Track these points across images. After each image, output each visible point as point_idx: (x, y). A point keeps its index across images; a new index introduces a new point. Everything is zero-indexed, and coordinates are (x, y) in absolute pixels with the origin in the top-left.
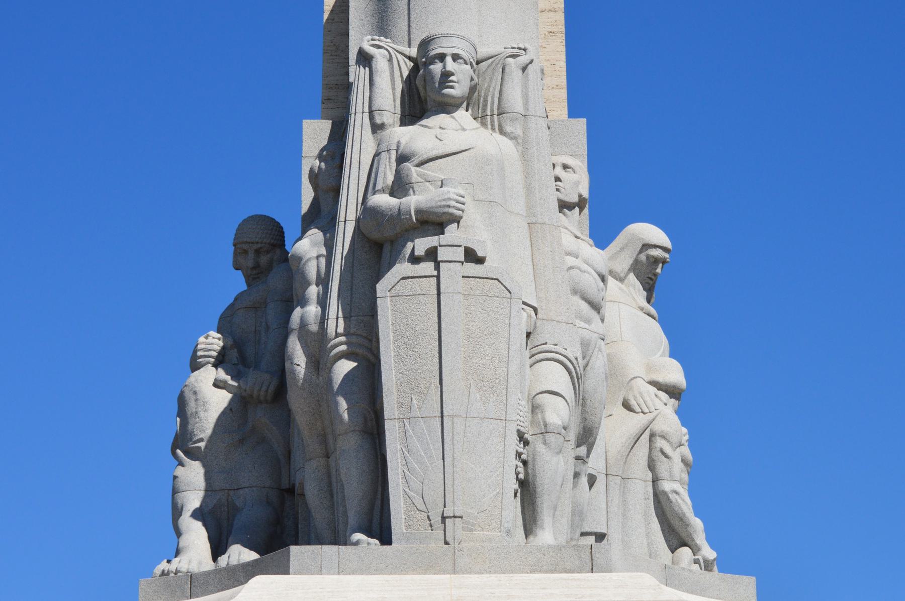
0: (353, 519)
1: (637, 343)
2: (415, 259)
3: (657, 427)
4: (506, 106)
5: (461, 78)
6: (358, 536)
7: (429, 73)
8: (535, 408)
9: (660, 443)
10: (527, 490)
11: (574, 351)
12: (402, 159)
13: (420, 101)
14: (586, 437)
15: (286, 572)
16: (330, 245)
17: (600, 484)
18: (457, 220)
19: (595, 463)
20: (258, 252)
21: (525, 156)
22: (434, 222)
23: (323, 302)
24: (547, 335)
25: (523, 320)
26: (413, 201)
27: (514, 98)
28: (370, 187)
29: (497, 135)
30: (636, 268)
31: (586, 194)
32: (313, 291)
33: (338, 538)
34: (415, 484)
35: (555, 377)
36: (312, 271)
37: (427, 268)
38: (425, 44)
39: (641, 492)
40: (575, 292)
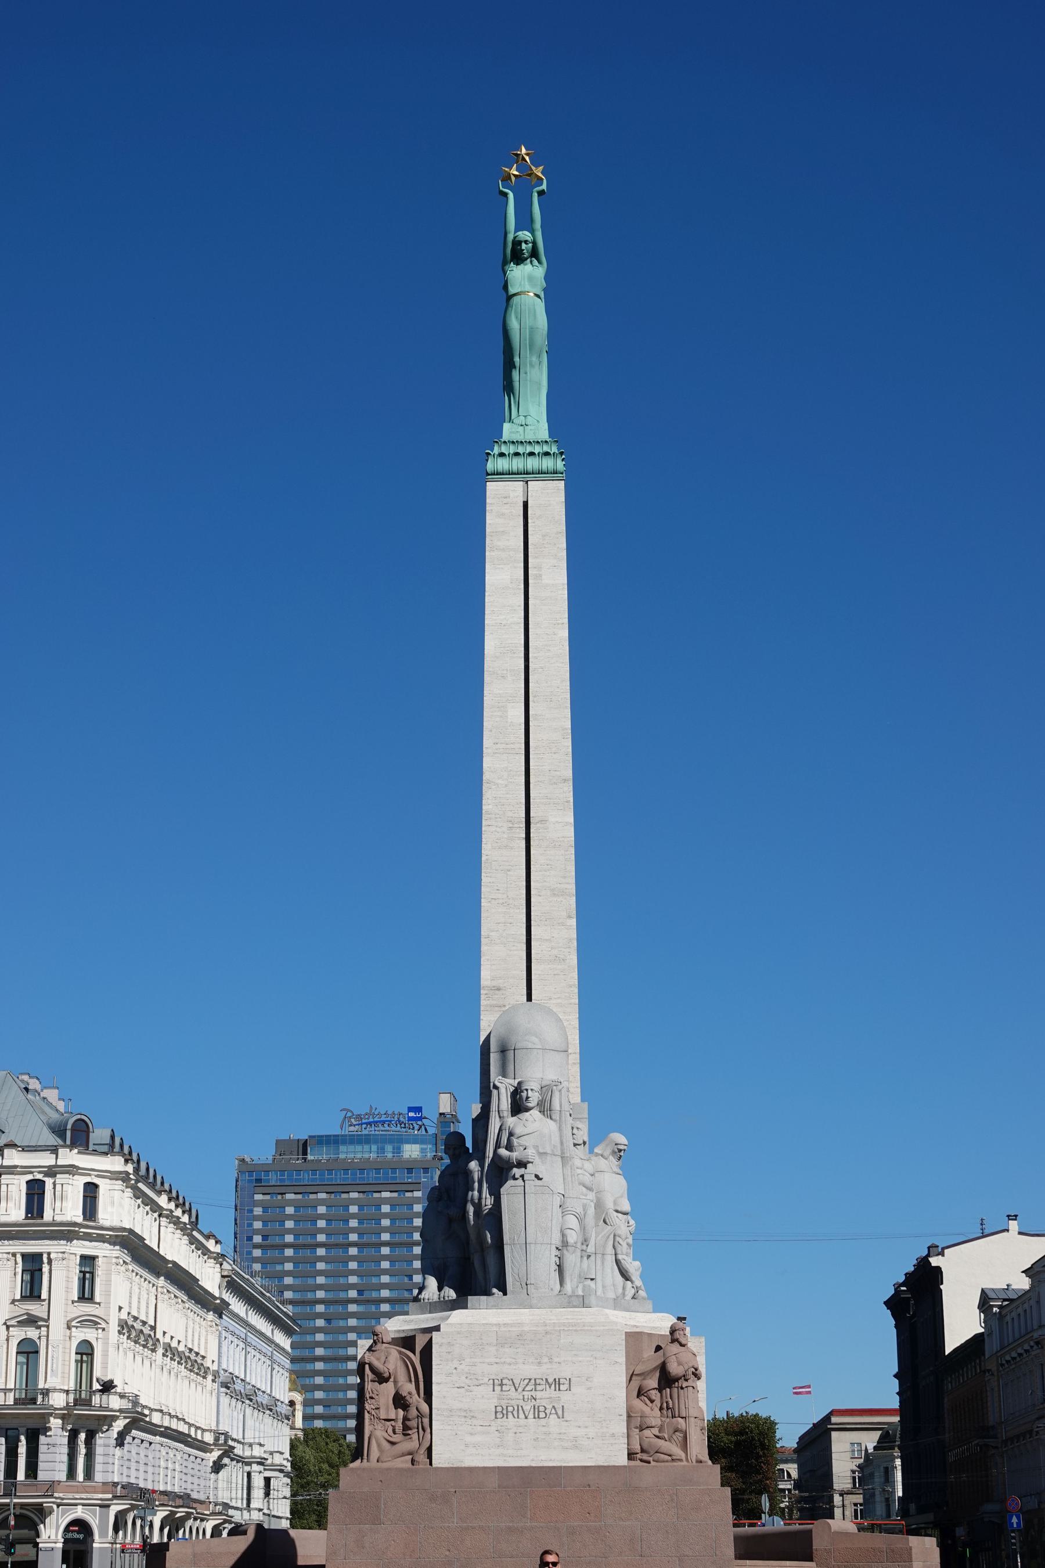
0: (492, 1283)
1: (614, 1186)
2: (515, 1178)
3: (619, 1232)
4: (553, 1108)
5: (534, 1098)
6: (495, 1290)
7: (521, 1097)
8: (563, 1235)
9: (618, 1239)
10: (560, 1268)
11: (580, 1210)
12: (511, 1134)
13: (518, 1107)
14: (585, 1241)
15: (466, 1308)
16: (482, 1166)
17: (592, 1258)
18: (505, 1294)
19: (591, 1249)
20: (455, 1149)
21: (560, 1129)
22: (522, 1164)
23: (480, 1191)
24: (569, 1204)
25: (558, 1200)
26: (515, 1155)
27: (556, 1105)
28: (498, 1145)
29: (549, 1120)
30: (614, 1152)
31: (586, 1139)
32: (476, 1185)
33: (488, 1293)
34: (516, 1271)
35: (572, 1222)
36: (476, 1178)
37: (520, 1182)
38: (520, 1083)
39: (610, 1259)
40: (580, 1184)
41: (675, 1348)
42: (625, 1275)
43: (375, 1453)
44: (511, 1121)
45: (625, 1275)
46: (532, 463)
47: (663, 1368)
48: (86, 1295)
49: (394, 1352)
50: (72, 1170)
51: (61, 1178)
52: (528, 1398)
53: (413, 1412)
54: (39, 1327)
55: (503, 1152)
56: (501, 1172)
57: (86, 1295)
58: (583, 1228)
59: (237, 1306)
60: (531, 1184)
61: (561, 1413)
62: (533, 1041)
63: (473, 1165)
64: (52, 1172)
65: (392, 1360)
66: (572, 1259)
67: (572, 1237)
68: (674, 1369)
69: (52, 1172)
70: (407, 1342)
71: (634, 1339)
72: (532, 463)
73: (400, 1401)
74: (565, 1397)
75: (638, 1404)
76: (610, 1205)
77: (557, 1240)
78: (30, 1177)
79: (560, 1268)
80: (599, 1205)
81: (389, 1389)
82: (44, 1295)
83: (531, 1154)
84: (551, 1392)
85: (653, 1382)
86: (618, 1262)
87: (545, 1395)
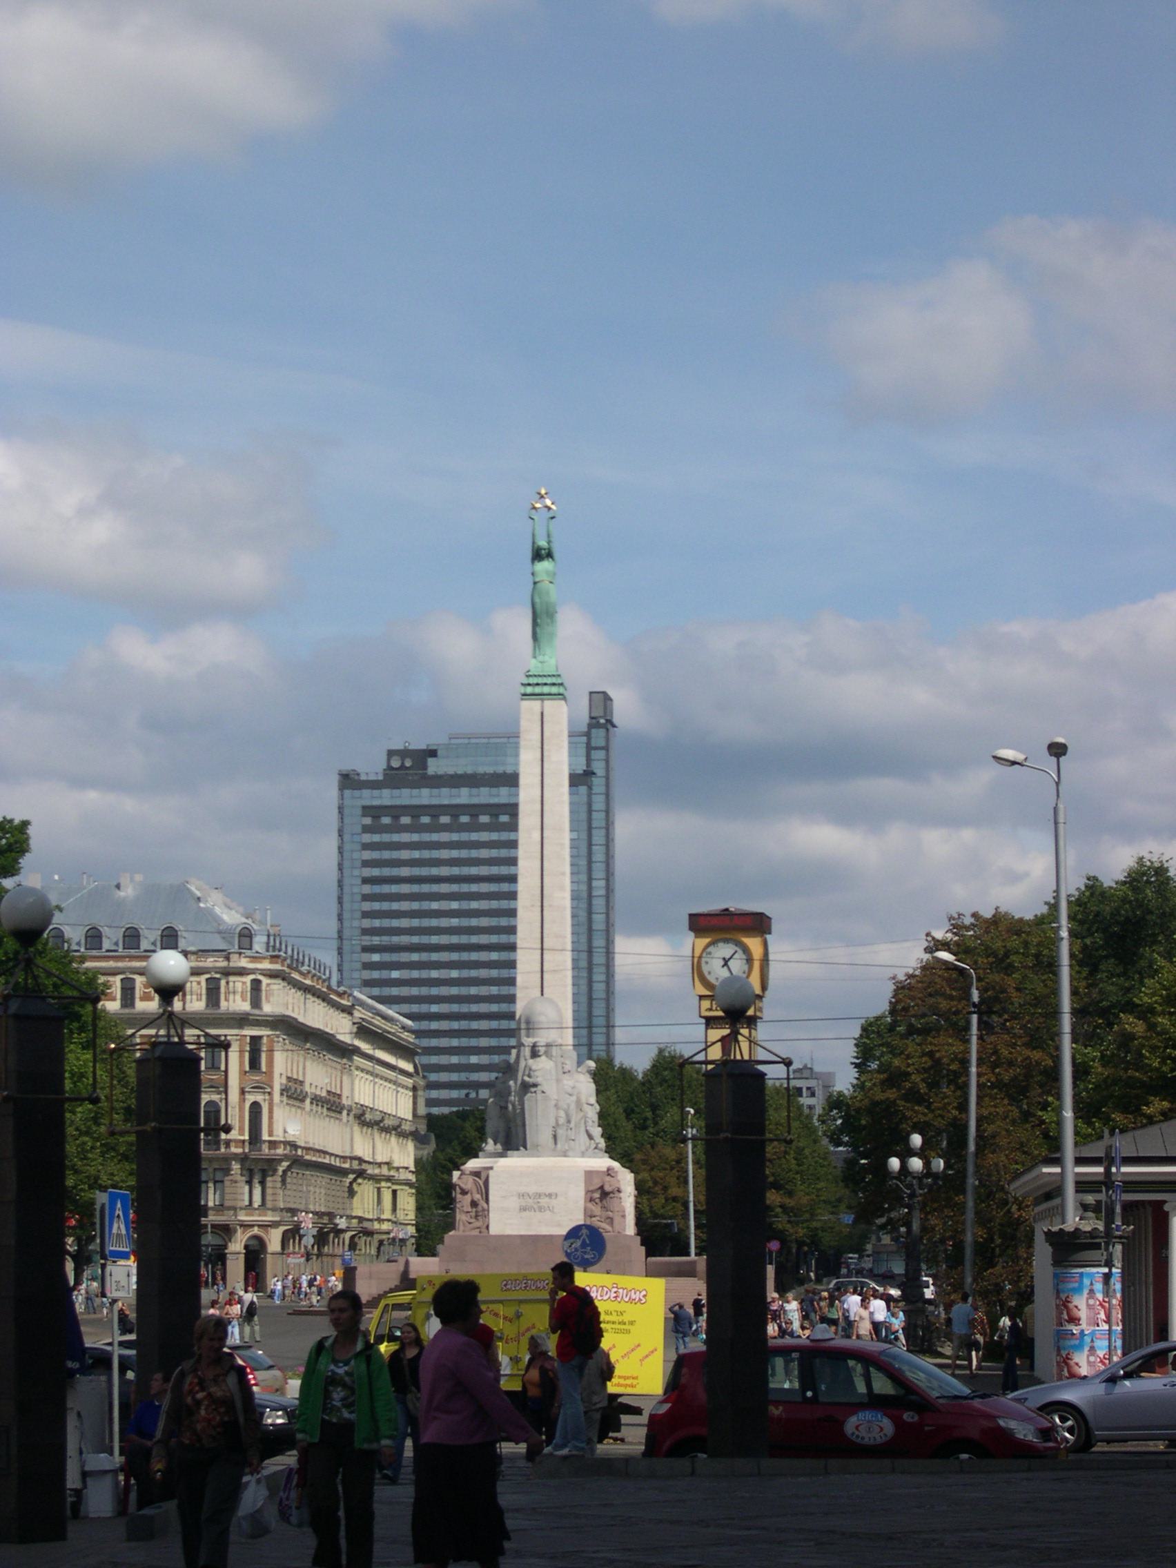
5: (542, 1050)
10: (555, 1137)
13: (535, 1054)
14: (569, 1122)
19: (572, 1125)
22: (535, 1085)
35: (562, 1114)
39: (583, 1129)
41: (608, 1178)
42: (591, 1137)
43: (462, 1228)
44: (531, 1062)
45: (591, 1137)
46: (546, 689)
47: (602, 1188)
48: (254, 1064)
49: (471, 1179)
50: (242, 972)
51: (232, 978)
52: (534, 1202)
53: (480, 1208)
54: (219, 1093)
55: (526, 1078)
56: (526, 1087)
57: (254, 1064)
58: (567, 1115)
59: (365, 1047)
60: (540, 1096)
61: (551, 1209)
62: (542, 1019)
63: (511, 1083)
64: (227, 973)
65: (468, 1183)
66: (560, 1132)
67: (562, 1121)
68: (607, 1188)
69: (227, 973)
70: (477, 1174)
71: (589, 1174)
72: (546, 689)
73: (474, 1204)
74: (554, 1202)
75: (590, 1205)
76: (583, 1100)
77: (553, 1123)
78: (208, 976)
79: (555, 1137)
80: (578, 1102)
81: (468, 1198)
82: (223, 1068)
83: (539, 1080)
84: (547, 1199)
85: (597, 1195)
86: (587, 1131)
87: (544, 1201)
